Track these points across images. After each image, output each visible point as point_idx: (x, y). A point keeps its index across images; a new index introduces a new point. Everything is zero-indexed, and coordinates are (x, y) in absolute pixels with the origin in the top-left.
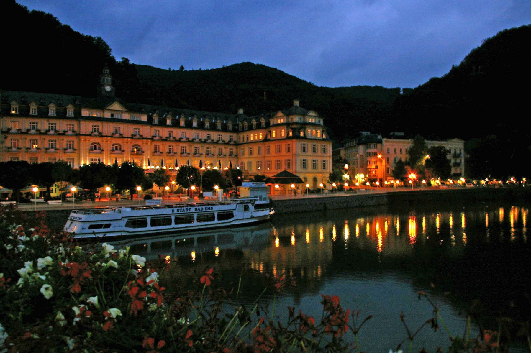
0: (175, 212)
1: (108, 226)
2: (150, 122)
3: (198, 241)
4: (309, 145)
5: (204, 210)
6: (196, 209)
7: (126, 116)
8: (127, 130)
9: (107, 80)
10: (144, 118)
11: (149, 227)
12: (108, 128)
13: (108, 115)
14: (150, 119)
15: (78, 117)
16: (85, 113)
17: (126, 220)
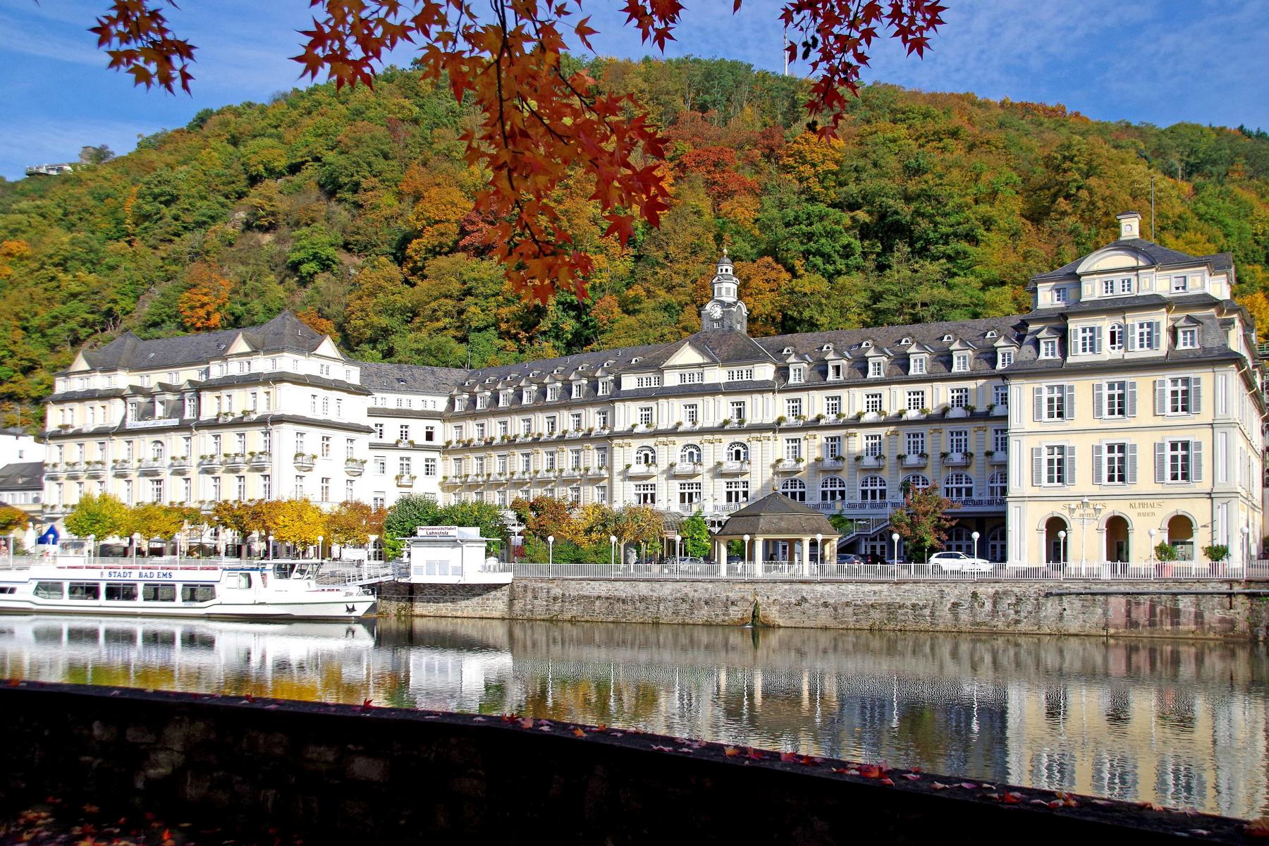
0: (106, 576)
1: (12, 591)
2: (781, 383)
3: (184, 641)
4: (1082, 390)
5: (155, 578)
6: (140, 575)
7: (717, 375)
8: (717, 410)
9: (728, 290)
10: (765, 372)
11: (65, 601)
12: (671, 412)
13: (672, 379)
14: (783, 372)
15: (619, 395)
16: (630, 382)
17: (35, 583)
